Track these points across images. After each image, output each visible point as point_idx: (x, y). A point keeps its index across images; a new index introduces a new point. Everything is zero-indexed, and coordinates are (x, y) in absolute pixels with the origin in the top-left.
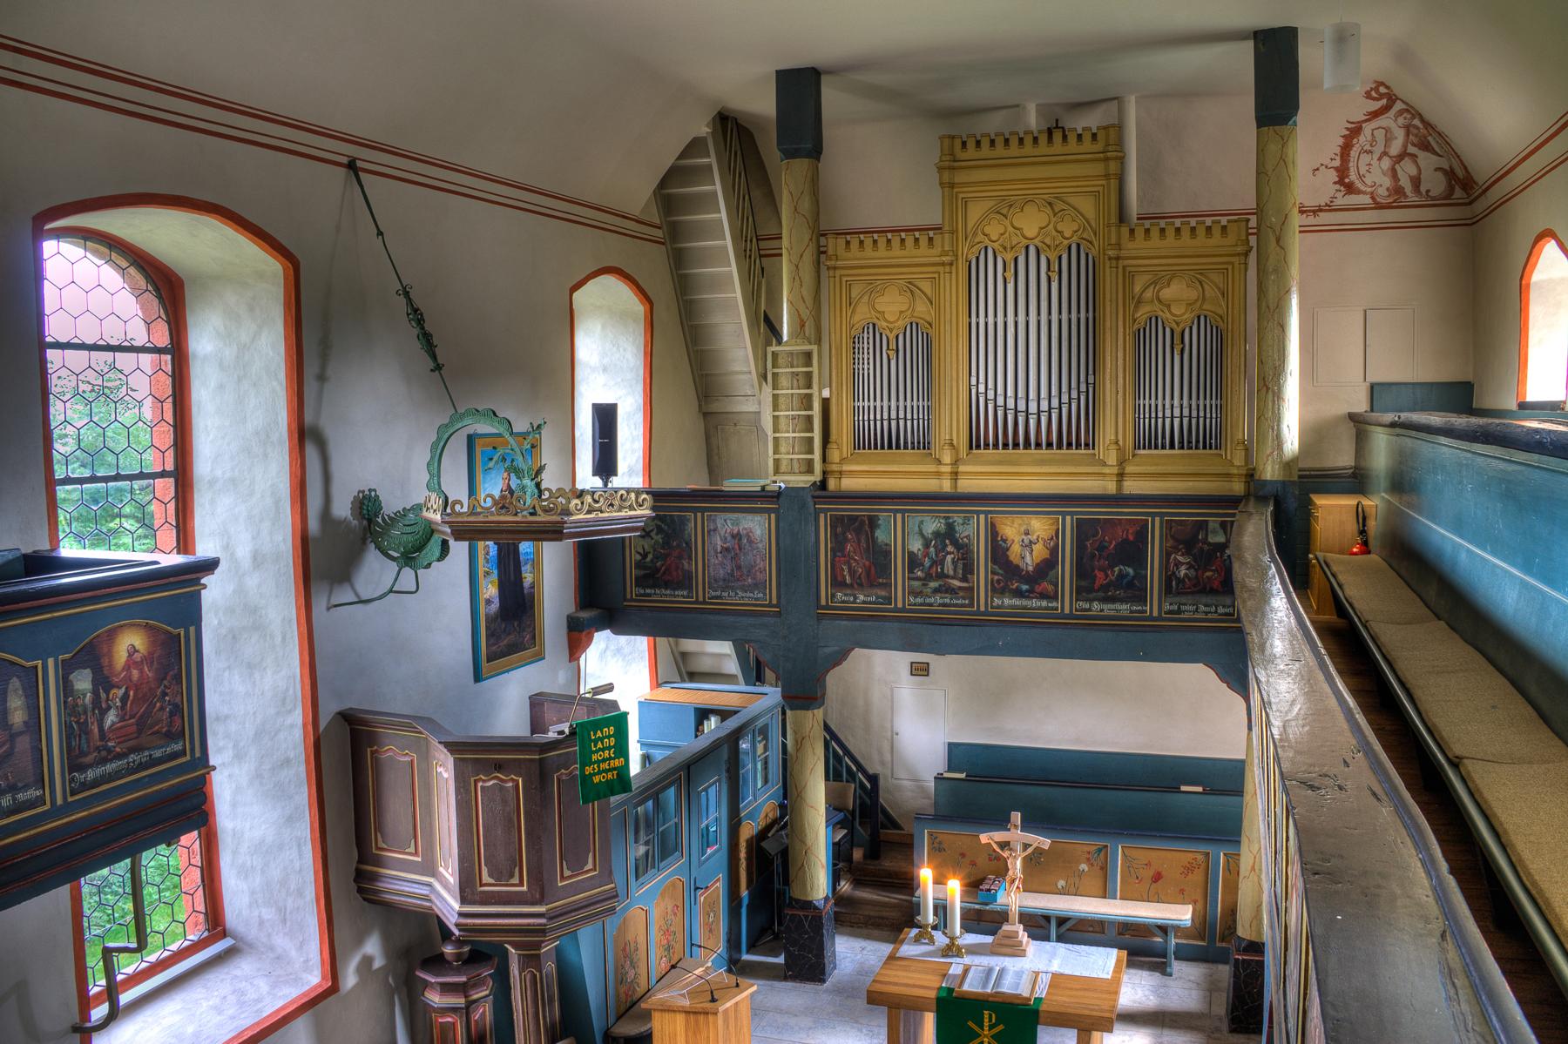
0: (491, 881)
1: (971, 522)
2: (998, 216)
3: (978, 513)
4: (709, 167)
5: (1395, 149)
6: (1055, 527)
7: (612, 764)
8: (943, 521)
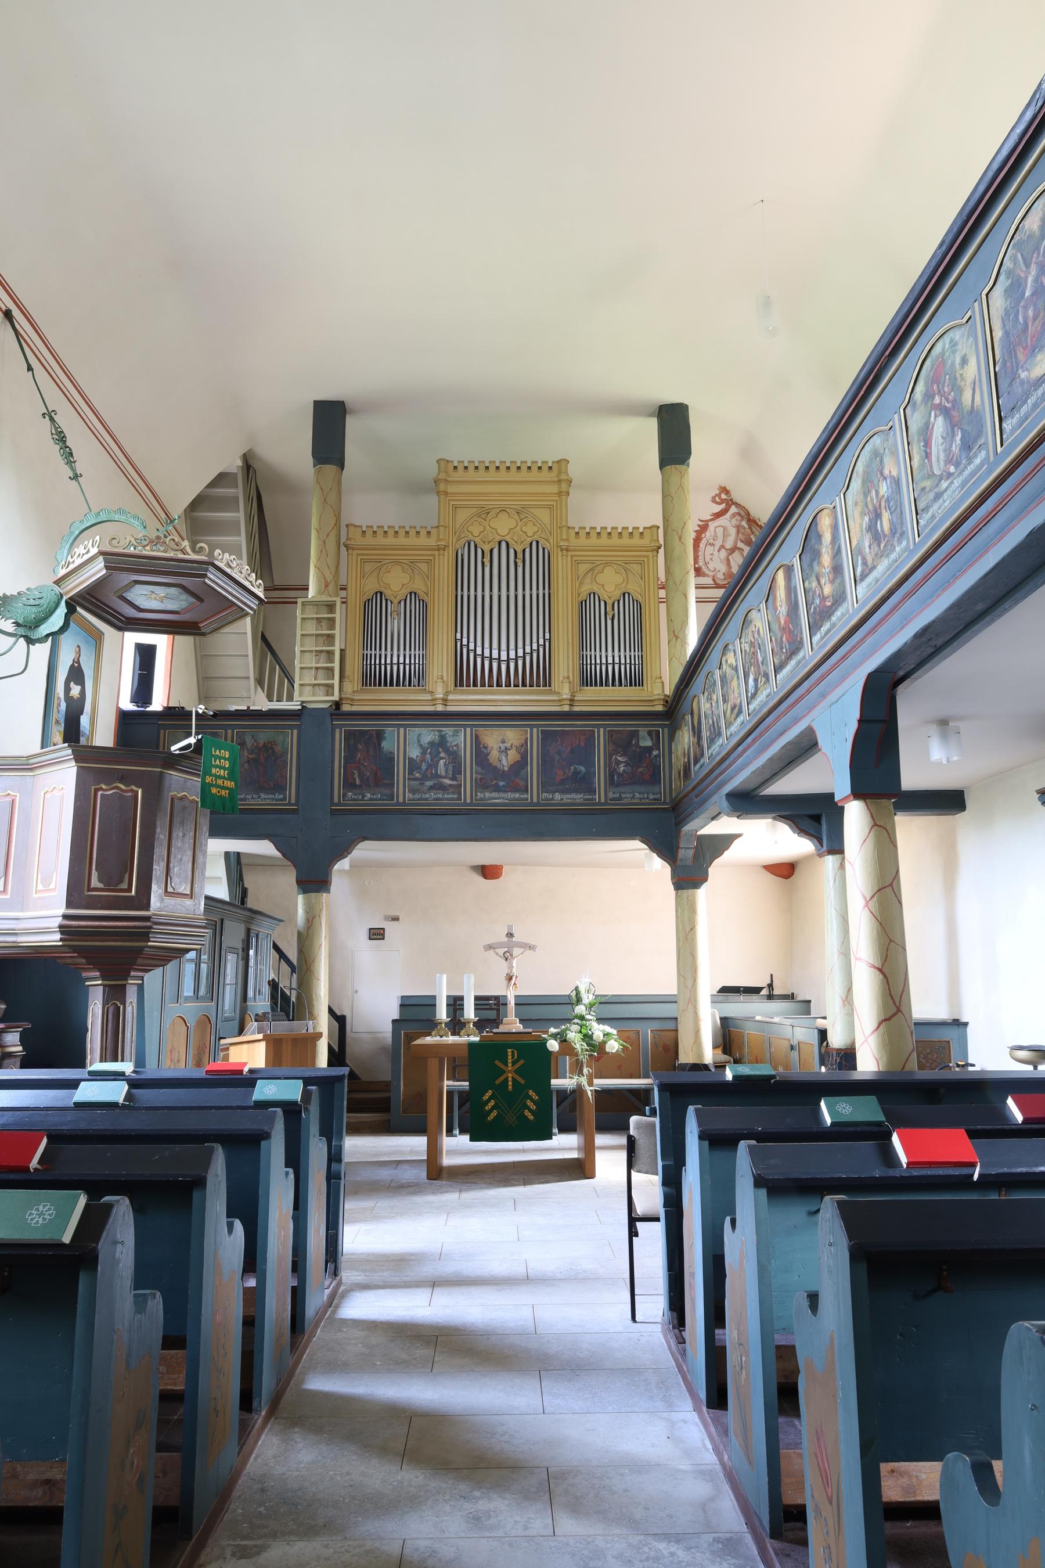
0: (101, 886)
1: (459, 734)
2: (479, 519)
3: (465, 726)
4: (236, 499)
5: (729, 545)
6: (524, 737)
7: (225, 783)
8: (436, 733)
